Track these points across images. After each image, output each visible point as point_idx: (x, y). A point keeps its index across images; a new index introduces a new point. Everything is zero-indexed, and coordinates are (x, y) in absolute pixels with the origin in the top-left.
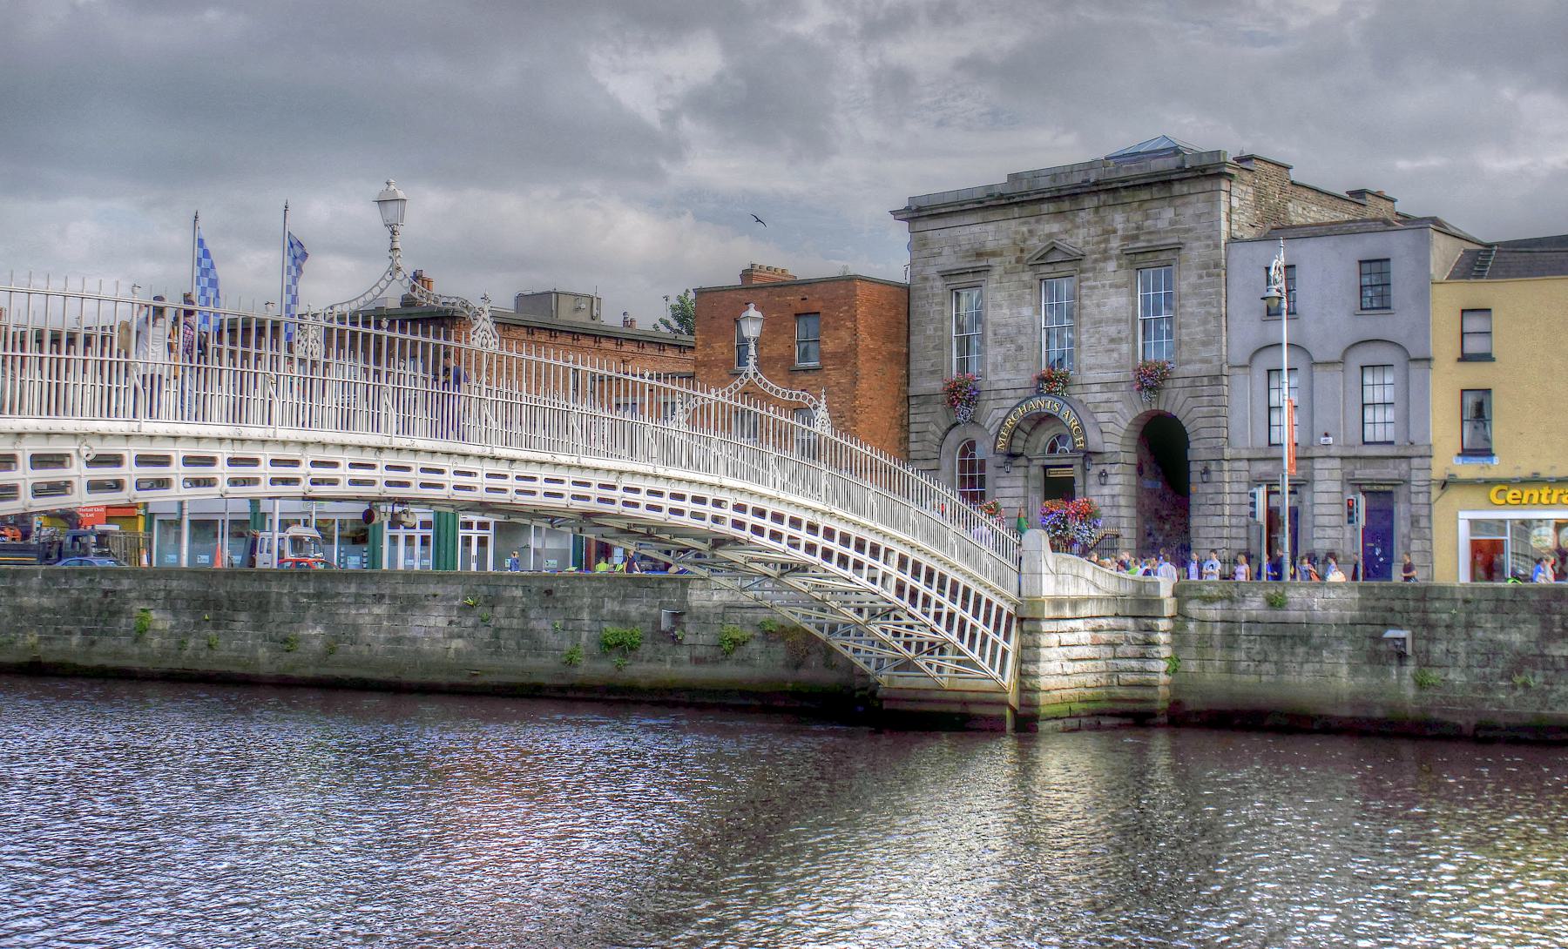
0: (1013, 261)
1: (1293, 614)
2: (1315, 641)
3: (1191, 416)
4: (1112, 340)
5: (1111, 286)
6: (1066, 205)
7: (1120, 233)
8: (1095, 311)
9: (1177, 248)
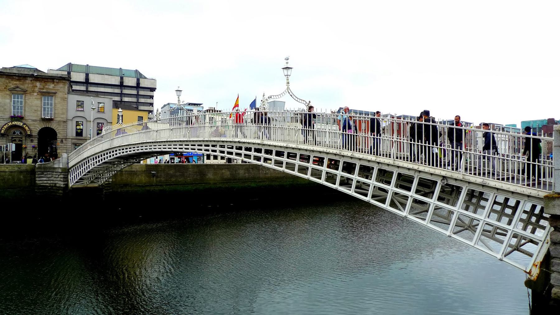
0: (3, 88)
1: (133, 170)
2: (138, 174)
3: (58, 129)
4: (35, 111)
5: (35, 98)
6: (22, 78)
7: (38, 87)
8: (30, 103)
9: (55, 93)
